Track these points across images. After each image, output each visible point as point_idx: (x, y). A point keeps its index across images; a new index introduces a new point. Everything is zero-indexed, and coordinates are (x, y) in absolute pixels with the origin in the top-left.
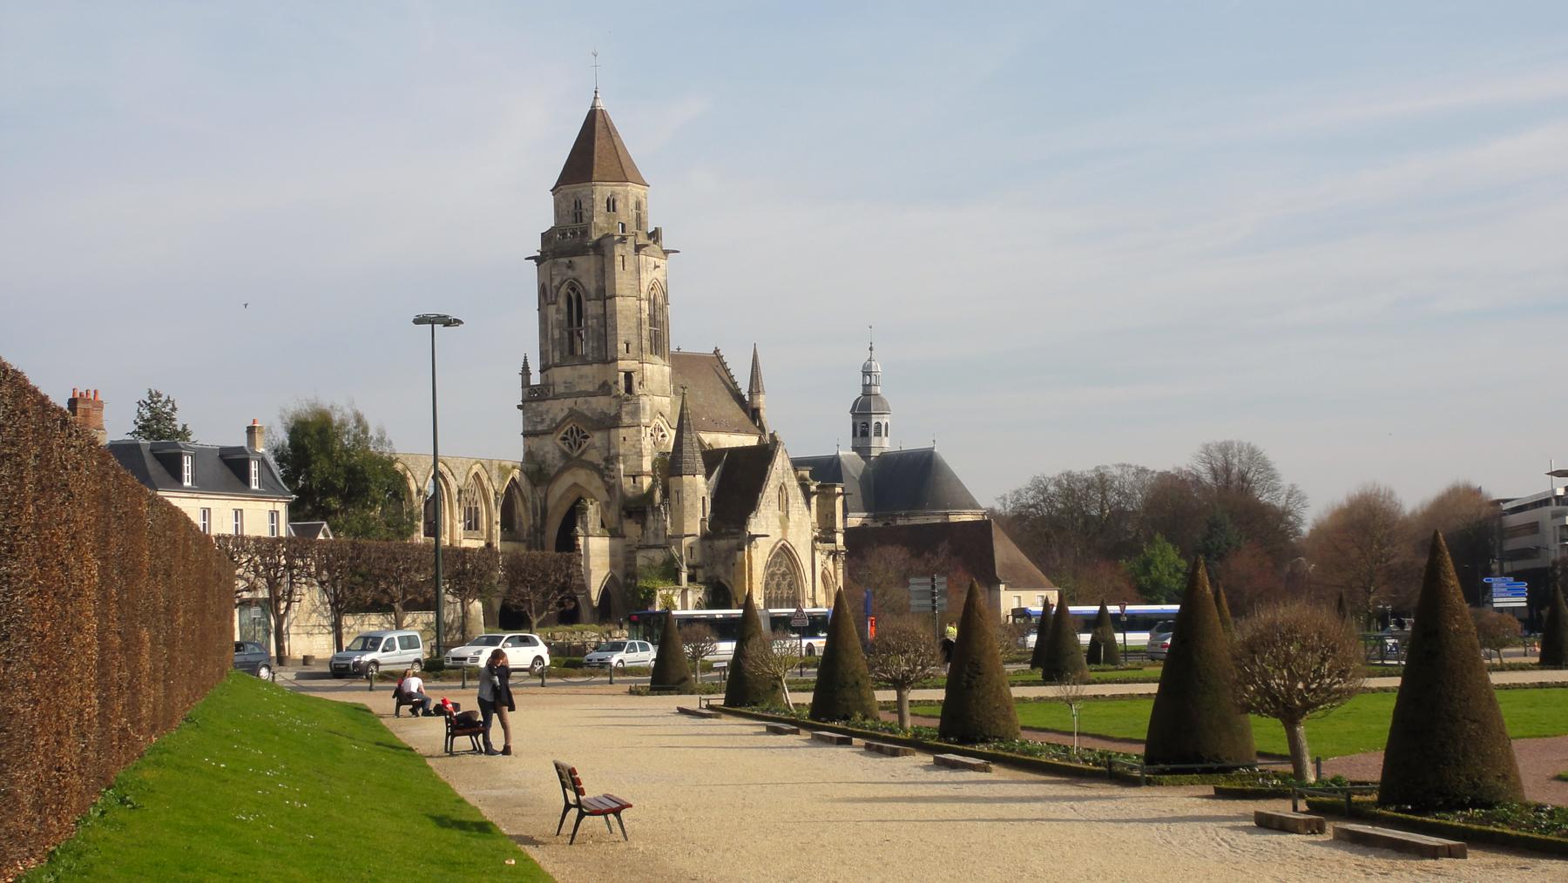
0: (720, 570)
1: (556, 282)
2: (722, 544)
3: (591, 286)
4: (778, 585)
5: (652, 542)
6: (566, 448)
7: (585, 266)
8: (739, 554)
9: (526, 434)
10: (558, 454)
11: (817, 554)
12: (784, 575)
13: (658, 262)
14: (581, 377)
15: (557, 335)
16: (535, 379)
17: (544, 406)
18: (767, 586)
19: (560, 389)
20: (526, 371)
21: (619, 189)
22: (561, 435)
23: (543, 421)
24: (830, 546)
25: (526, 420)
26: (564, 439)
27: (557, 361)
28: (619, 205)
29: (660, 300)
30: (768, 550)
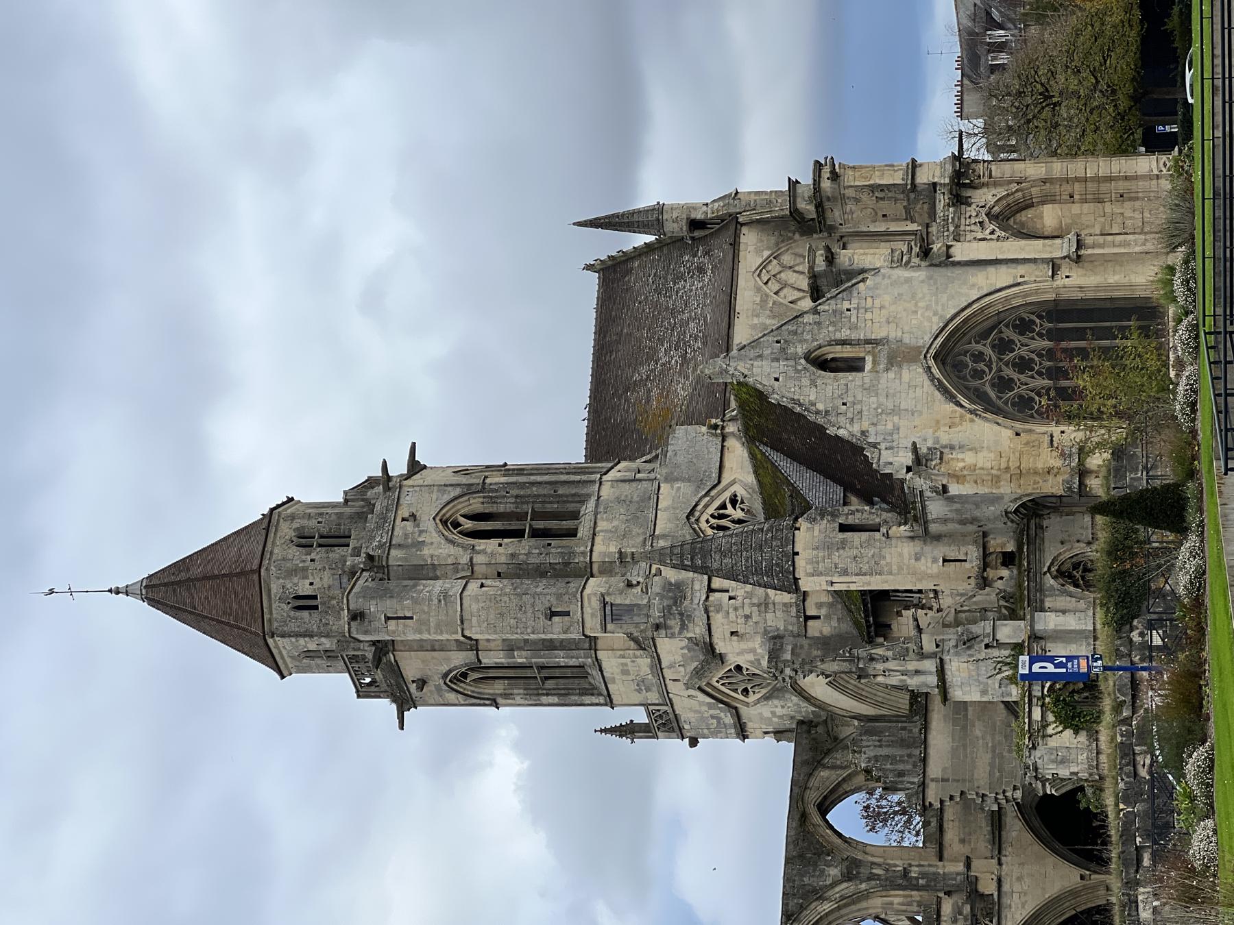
0: (993, 510)
1: (452, 696)
2: (936, 508)
3: (459, 659)
4: (1023, 365)
5: (933, 680)
6: (764, 691)
7: (411, 666)
8: (954, 489)
9: (743, 734)
10: (776, 702)
11: (961, 252)
12: (1003, 346)
13: (404, 512)
14: (625, 672)
15: (555, 699)
16: (640, 716)
17: (685, 715)
18: (1022, 409)
19: (653, 697)
20: (628, 731)
21: (275, 588)
22: (742, 698)
23: (712, 717)
24: (942, 200)
25: (714, 734)
26: (745, 692)
27: (602, 700)
28: (304, 588)
29: (476, 504)
30: (952, 407)
